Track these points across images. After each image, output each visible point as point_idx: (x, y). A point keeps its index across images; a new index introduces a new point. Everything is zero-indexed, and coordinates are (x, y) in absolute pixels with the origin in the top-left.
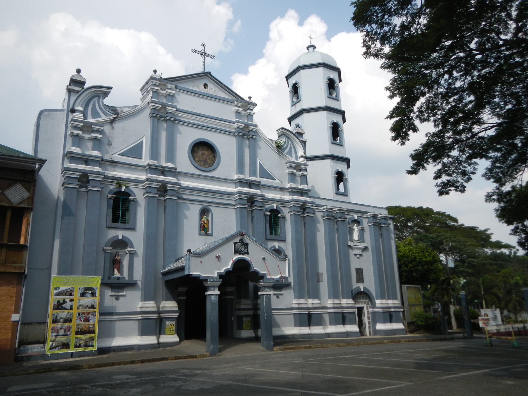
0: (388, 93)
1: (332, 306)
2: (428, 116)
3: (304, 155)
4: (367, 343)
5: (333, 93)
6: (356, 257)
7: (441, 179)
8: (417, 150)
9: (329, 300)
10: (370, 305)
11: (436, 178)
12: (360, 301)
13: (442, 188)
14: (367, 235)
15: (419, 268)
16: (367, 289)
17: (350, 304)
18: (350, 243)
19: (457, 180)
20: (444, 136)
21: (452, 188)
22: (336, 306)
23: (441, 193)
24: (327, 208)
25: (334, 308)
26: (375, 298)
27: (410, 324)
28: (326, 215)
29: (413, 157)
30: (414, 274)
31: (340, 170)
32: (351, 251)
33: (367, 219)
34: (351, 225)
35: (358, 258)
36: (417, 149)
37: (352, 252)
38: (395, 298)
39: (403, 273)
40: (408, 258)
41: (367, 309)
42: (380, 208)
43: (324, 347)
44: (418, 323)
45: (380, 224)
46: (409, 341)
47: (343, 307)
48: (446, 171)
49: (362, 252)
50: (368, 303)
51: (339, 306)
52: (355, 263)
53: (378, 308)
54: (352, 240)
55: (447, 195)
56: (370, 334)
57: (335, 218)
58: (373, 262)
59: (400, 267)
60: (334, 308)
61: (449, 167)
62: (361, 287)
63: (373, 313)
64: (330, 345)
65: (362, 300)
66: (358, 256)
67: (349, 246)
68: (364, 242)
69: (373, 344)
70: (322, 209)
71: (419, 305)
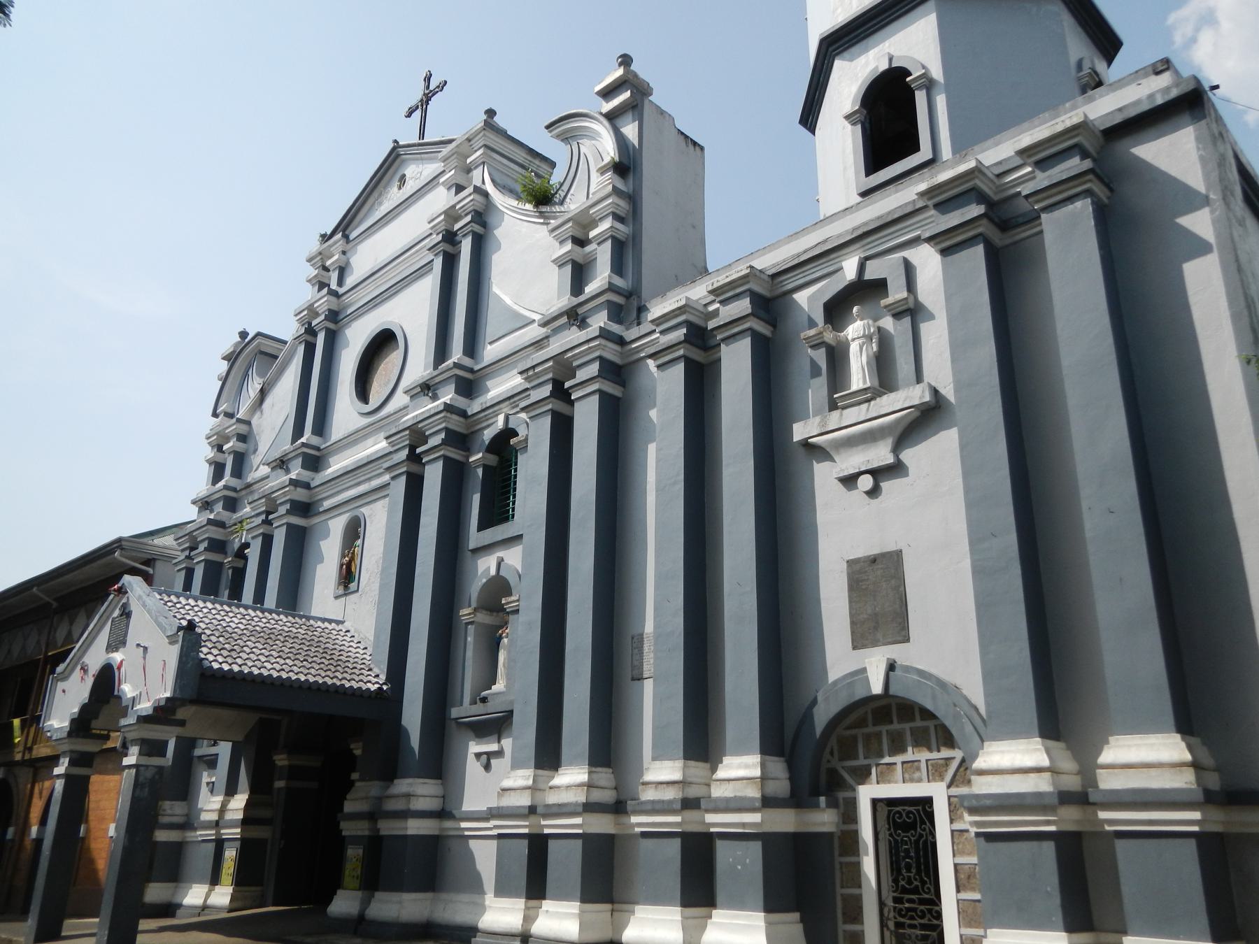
12: (898, 759)
37: (825, 476)
65: (910, 755)
66: (866, 482)
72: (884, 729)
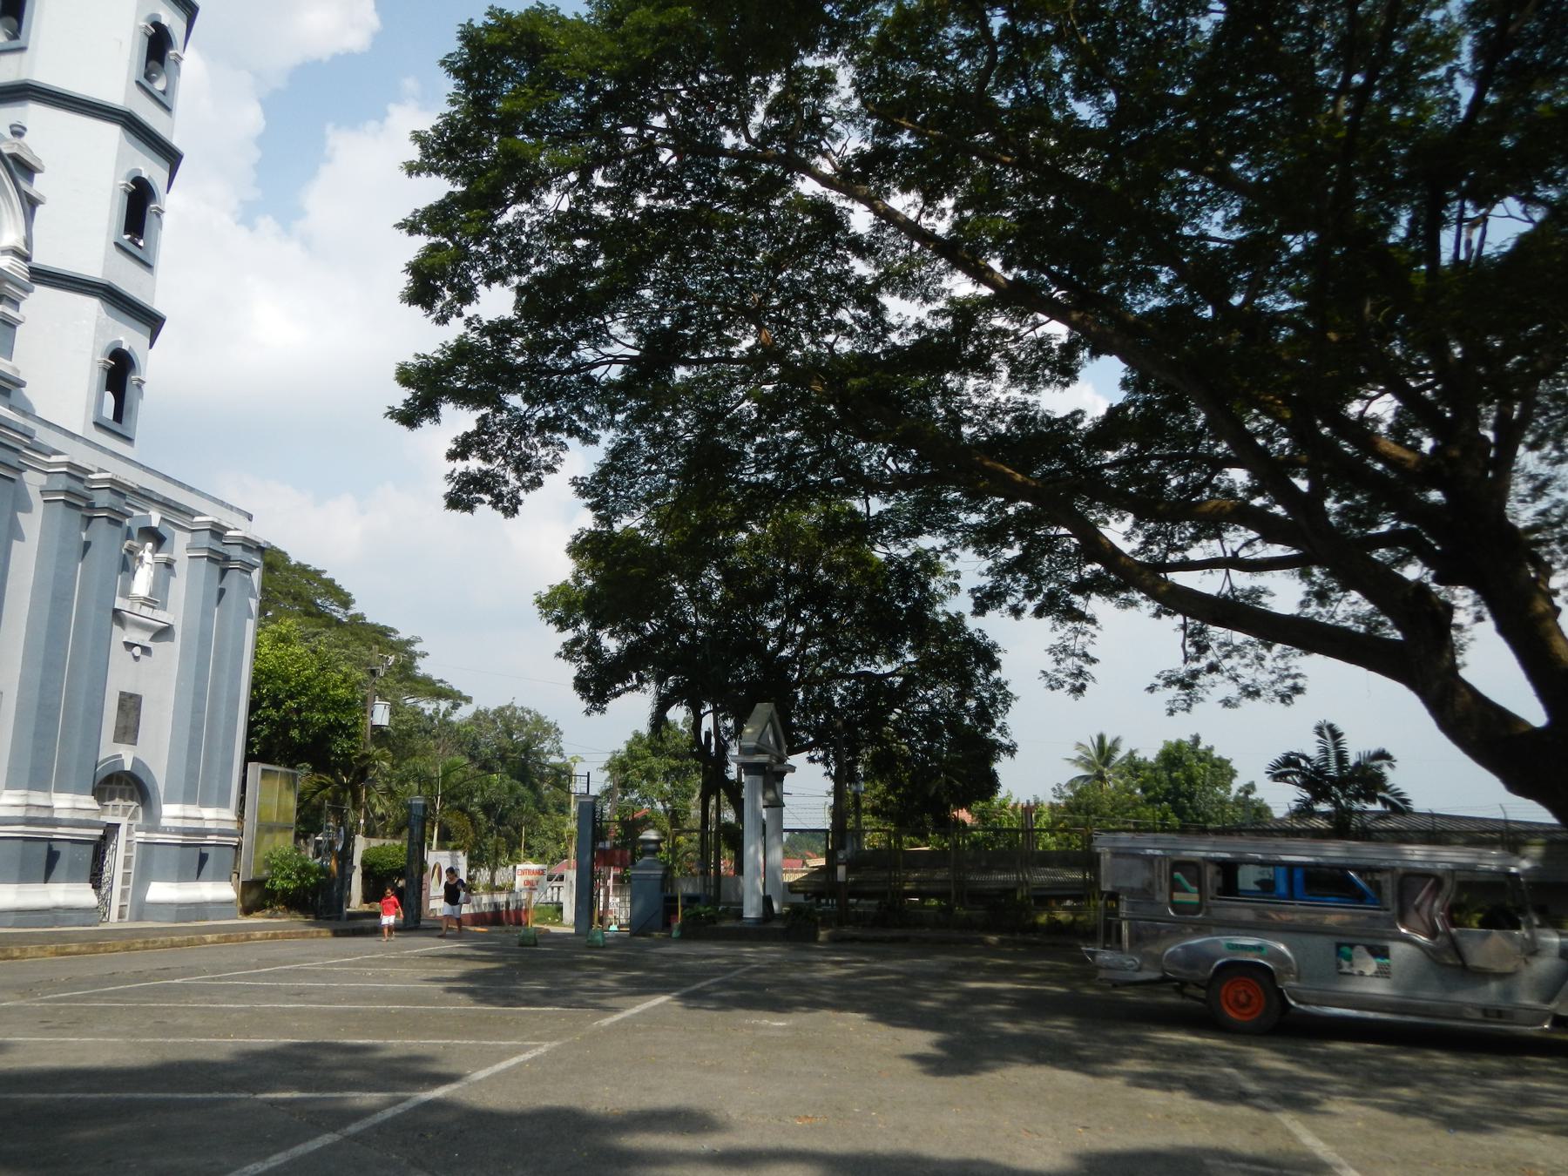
0: (415, 153)
1: (19, 812)
2: (509, 266)
3: (24, 249)
4: (155, 942)
5: (159, 75)
6: (129, 654)
7: (466, 463)
8: (425, 357)
9: (7, 792)
10: (140, 821)
11: (452, 456)
12: (110, 803)
13: (459, 490)
14: (179, 586)
15: (316, 716)
16: (144, 765)
17: (84, 813)
18: (119, 603)
19: (503, 477)
20: (509, 341)
21: (487, 498)
22: (33, 813)
23: (454, 502)
24: (70, 465)
25: (29, 821)
26: (162, 796)
27: (247, 887)
28: (60, 487)
29: (405, 376)
30: (295, 733)
31: (125, 347)
32: (116, 628)
33: (188, 535)
34: (135, 544)
35: (136, 658)
36: (429, 353)
38: (223, 803)
39: (259, 728)
40: (286, 681)
41: (129, 833)
42: (232, 508)
43: (12, 958)
44: (273, 884)
45: (227, 559)
46: (275, 937)
47: (56, 819)
48: (484, 443)
49: (151, 640)
50: (136, 811)
51: (44, 814)
52: (122, 675)
53: (170, 833)
54: (126, 594)
55: (467, 514)
56: (121, 916)
57: (91, 507)
58: (179, 679)
59: (254, 706)
60: (29, 821)
61: (493, 434)
62: (127, 757)
63: (146, 845)
64: (32, 949)
65: (117, 801)
66: (137, 651)
67: (116, 612)
68: (164, 608)
69: (173, 945)
70: (49, 465)
71: (286, 829)
72: (109, 786)
